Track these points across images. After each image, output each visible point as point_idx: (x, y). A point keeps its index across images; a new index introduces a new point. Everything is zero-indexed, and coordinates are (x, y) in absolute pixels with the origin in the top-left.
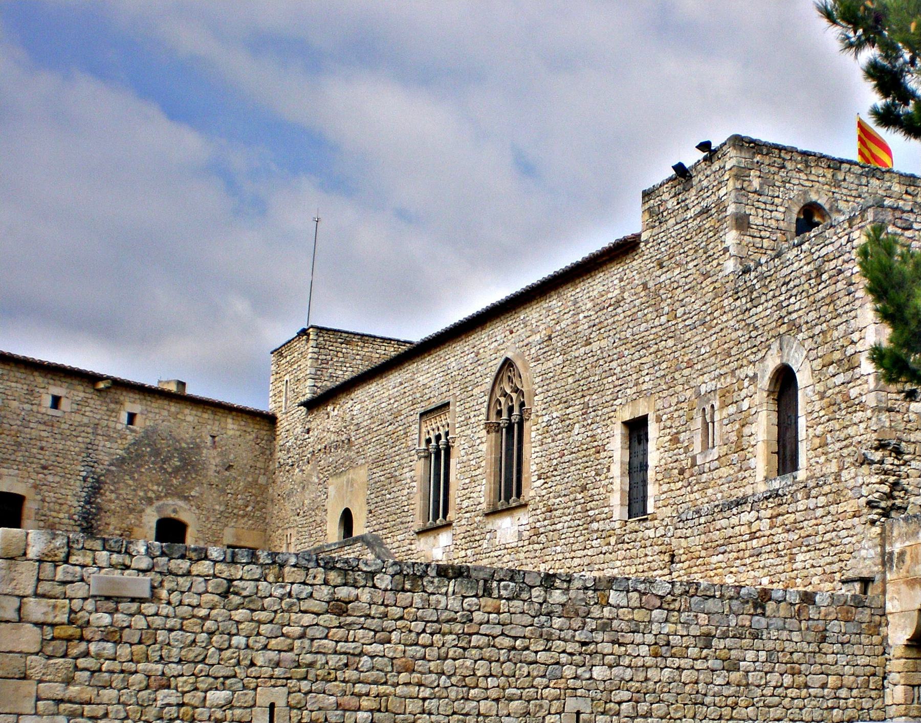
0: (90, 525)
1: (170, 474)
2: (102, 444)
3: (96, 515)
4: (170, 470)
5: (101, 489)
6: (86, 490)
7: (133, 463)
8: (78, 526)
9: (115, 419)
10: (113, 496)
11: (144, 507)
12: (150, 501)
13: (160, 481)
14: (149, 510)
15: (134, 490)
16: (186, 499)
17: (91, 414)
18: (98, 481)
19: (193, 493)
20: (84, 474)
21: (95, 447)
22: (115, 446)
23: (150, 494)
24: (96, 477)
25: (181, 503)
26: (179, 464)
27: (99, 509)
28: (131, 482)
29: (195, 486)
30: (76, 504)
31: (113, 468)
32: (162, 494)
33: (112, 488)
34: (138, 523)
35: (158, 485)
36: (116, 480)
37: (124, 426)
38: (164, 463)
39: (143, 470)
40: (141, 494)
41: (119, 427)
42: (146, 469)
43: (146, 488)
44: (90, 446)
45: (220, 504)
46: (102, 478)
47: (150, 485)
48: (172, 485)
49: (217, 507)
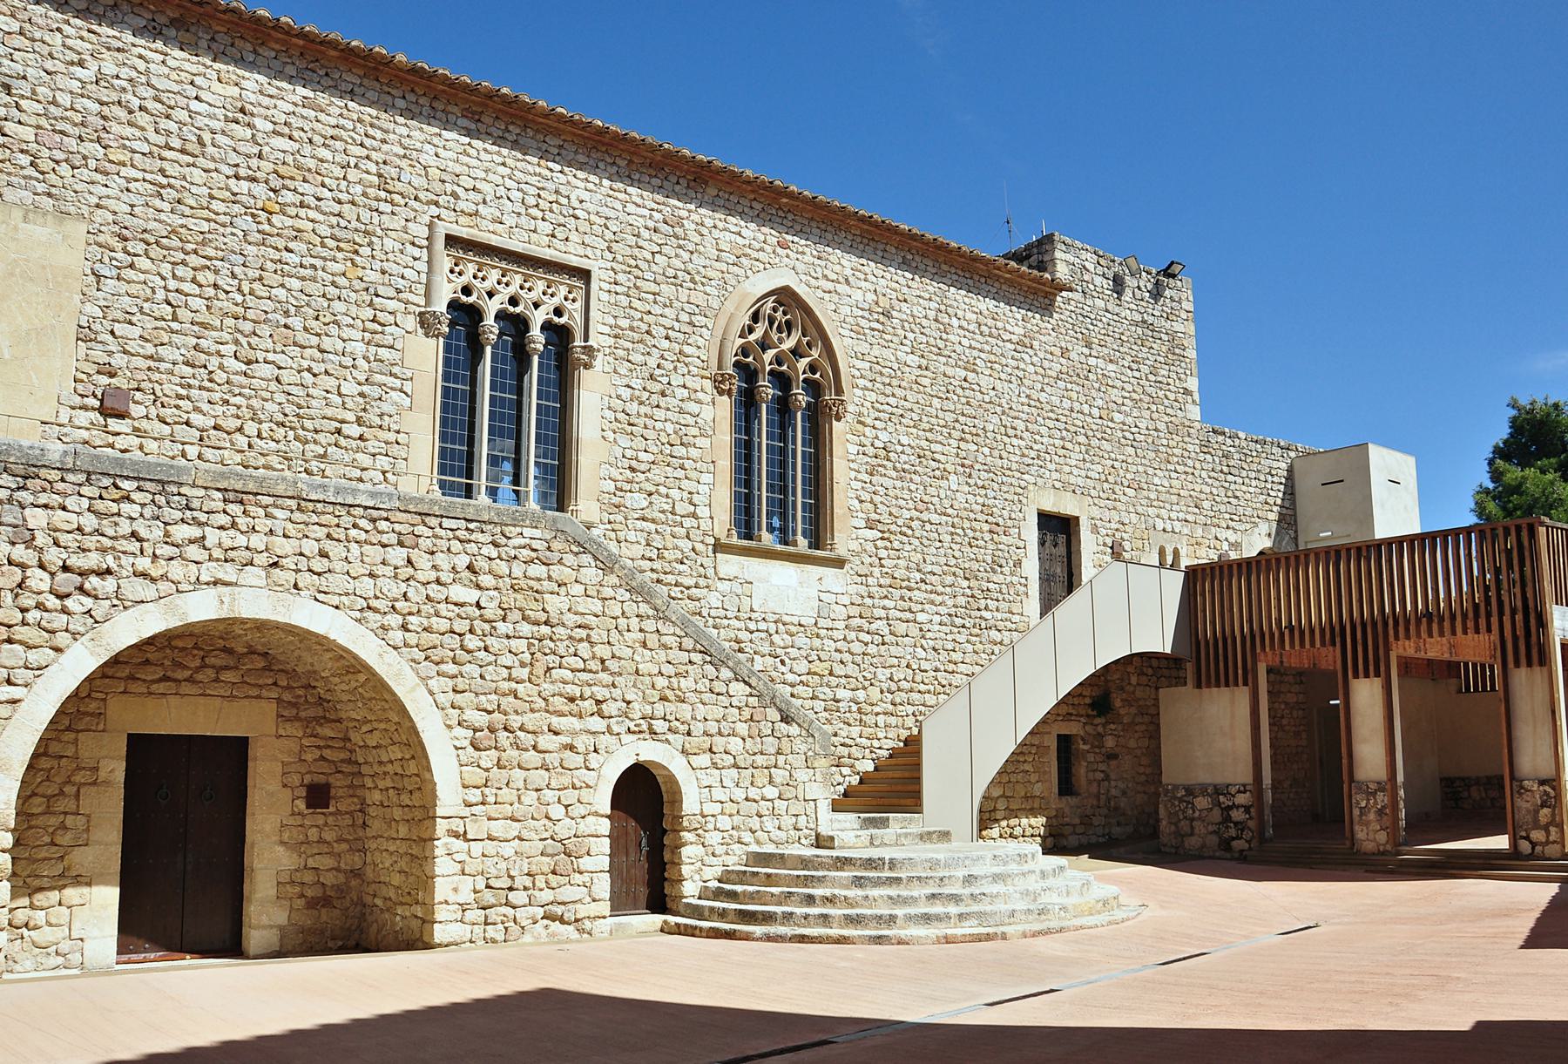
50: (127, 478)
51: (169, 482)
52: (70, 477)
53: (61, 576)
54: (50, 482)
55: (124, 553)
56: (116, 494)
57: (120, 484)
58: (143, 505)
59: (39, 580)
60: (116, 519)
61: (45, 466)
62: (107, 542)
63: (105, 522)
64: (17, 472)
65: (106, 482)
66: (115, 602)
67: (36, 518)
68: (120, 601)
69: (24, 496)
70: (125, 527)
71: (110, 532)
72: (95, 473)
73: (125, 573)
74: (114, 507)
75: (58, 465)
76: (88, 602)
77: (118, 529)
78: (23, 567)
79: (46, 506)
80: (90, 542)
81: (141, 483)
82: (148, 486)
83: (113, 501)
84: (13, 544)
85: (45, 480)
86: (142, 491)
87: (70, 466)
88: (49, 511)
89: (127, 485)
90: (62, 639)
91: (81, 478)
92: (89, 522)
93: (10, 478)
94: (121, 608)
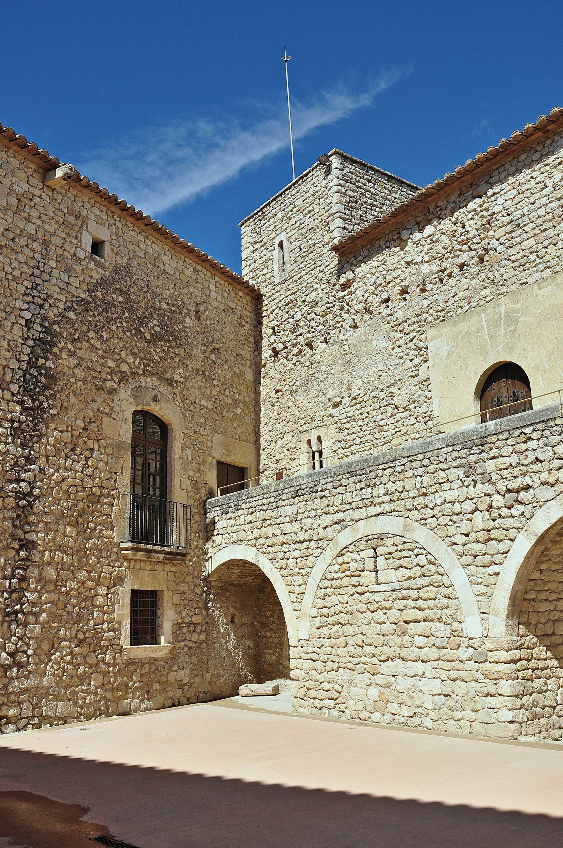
0: (37, 403)
1: (149, 342)
2: (55, 273)
3: (45, 387)
4: (148, 336)
5: (54, 345)
6: (30, 343)
7: (100, 314)
8: (17, 402)
9: (75, 242)
10: (73, 361)
11: (115, 386)
12: (123, 378)
13: (137, 351)
14: (124, 393)
15: (103, 357)
16: (169, 382)
17: (39, 223)
18: (48, 330)
19: (177, 378)
20: (28, 316)
21: (45, 277)
22: (75, 282)
23: (124, 368)
24: (47, 324)
25: (163, 388)
26: (159, 330)
27: (51, 377)
28: (97, 344)
29: (178, 367)
30: (14, 365)
31: (72, 315)
32: (140, 371)
33: (69, 346)
34: (107, 410)
35: (135, 355)
36: (76, 336)
37: (87, 254)
38: (141, 324)
39: (114, 328)
40: (111, 363)
41: (81, 254)
42: (118, 328)
43: (118, 357)
44: (37, 272)
45: (208, 399)
46: (55, 327)
47: (123, 354)
48: (151, 360)
49: (203, 402)
50: (527, 426)
51: (548, 420)
52: (501, 437)
53: (507, 495)
54: (493, 443)
55: (534, 472)
56: (523, 438)
57: (525, 431)
58: (538, 439)
59: (498, 501)
60: (527, 453)
61: (489, 435)
62: (524, 469)
63: (521, 457)
64: (478, 444)
65: (517, 433)
66: (535, 504)
67: (491, 466)
68: (538, 504)
69: (484, 456)
70: (532, 456)
71: (525, 462)
72: (511, 430)
73: (536, 485)
74: (524, 446)
75: (494, 432)
76: (521, 508)
77: (528, 459)
78: (489, 495)
79: (494, 458)
80: (516, 471)
81: (534, 426)
82: (538, 426)
83: (523, 442)
84: (484, 484)
85: (491, 443)
86: (536, 431)
87: (499, 431)
88: (496, 460)
89: (528, 430)
90: (512, 533)
91: (506, 435)
92: (514, 459)
93: (477, 448)
94: (538, 507)
